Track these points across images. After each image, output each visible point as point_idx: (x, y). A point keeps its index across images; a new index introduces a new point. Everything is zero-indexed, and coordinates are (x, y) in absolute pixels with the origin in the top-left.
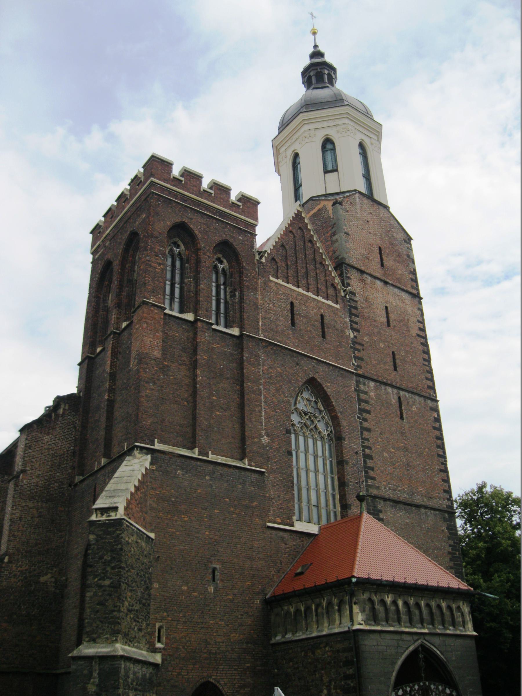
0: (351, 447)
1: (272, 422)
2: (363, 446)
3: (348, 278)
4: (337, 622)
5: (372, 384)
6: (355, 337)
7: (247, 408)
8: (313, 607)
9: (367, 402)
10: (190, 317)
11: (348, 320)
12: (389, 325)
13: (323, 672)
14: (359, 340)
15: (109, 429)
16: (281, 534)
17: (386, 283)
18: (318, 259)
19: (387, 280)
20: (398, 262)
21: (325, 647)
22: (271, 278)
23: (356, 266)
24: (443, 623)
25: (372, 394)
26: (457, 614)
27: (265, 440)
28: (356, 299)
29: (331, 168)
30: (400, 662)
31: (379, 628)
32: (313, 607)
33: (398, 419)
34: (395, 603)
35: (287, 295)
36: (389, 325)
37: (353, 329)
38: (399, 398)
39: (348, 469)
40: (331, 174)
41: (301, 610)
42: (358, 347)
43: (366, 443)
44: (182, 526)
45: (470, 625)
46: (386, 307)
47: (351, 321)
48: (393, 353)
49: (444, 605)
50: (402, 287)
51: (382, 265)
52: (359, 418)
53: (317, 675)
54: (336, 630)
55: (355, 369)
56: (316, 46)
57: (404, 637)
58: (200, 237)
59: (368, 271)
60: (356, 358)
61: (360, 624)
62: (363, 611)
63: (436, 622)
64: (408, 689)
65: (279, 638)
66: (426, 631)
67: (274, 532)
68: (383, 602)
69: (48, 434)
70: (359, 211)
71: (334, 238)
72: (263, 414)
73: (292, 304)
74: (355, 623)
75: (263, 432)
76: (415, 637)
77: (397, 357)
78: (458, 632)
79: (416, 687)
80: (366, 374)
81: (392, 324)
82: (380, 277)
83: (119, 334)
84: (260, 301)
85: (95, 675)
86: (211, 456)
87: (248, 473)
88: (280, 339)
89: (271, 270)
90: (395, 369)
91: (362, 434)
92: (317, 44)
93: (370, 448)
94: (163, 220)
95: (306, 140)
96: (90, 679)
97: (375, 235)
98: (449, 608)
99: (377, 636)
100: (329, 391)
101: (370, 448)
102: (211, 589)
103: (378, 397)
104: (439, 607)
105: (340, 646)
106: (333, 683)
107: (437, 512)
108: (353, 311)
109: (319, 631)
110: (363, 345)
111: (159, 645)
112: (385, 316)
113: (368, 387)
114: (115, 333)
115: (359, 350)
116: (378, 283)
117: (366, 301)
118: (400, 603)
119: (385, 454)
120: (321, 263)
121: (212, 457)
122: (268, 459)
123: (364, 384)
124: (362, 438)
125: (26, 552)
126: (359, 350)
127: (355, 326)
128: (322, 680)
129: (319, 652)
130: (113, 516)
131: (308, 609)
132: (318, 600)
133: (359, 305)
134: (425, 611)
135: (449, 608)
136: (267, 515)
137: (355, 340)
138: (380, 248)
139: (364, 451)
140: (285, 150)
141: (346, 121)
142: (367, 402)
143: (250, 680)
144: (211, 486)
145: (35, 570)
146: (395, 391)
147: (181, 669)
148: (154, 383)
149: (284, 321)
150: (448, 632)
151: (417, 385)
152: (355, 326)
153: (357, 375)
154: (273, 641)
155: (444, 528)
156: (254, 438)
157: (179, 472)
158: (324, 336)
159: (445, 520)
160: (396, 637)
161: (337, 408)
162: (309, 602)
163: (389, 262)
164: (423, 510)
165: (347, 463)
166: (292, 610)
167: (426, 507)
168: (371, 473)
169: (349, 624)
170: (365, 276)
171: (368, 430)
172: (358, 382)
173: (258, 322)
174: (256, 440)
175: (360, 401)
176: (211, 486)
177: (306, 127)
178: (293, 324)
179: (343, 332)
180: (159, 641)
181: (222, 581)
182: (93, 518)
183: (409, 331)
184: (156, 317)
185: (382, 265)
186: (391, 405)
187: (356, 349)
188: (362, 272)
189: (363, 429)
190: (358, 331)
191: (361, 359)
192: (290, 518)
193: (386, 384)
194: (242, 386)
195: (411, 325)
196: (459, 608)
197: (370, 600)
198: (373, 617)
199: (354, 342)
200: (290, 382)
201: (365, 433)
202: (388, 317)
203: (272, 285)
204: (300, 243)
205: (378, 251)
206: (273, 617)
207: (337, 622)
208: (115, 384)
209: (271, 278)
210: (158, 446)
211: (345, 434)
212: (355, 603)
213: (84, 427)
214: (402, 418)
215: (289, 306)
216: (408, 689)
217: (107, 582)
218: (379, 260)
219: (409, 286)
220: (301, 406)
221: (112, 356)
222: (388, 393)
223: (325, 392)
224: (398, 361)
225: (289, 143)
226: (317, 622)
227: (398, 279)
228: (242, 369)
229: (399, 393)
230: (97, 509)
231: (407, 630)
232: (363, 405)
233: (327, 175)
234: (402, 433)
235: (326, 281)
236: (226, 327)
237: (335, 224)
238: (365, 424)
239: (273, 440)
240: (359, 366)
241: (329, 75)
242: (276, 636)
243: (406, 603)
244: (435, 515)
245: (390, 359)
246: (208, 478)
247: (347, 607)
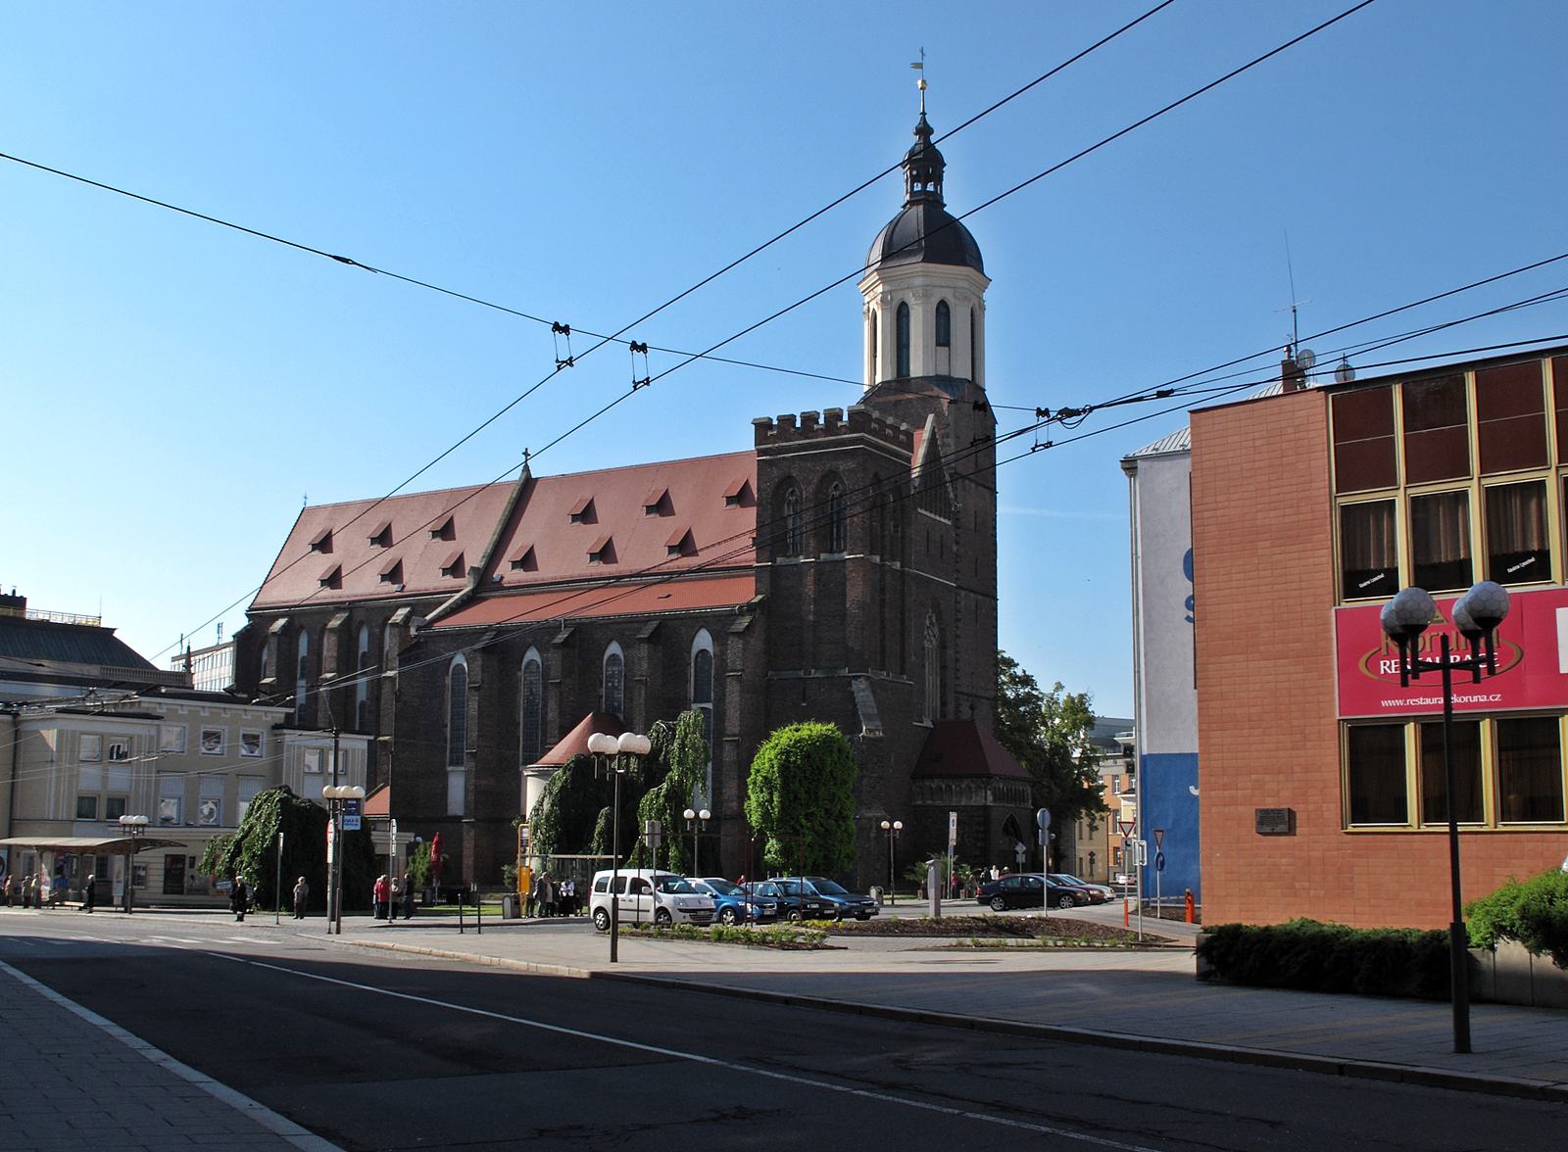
22: (919, 510)
25: (963, 603)
27: (913, 658)
29: (942, 341)
37: (957, 543)
42: (958, 560)
47: (956, 535)
56: (924, 113)
116: (973, 485)
142: (959, 611)
154: (913, 803)
168: (959, 675)
169: (983, 801)
175: (958, 611)
187: (957, 562)
192: (921, 716)
194: (902, 614)
198: (995, 800)
207: (974, 799)
209: (919, 510)
217: (875, 775)
228: (903, 601)
238: (958, 632)
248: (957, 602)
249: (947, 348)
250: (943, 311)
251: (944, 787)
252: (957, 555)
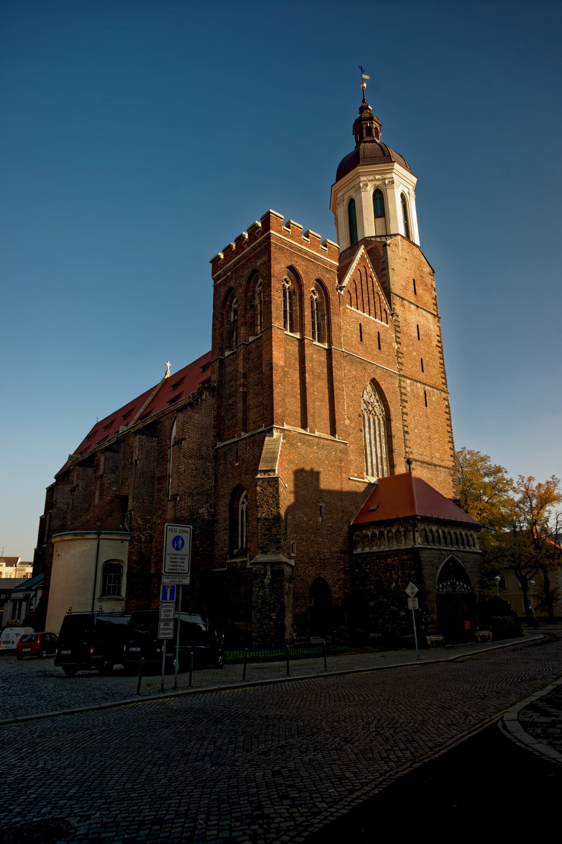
0: (396, 426)
1: (351, 409)
2: (403, 425)
3: (394, 303)
4: (404, 542)
5: (408, 381)
6: (398, 348)
7: (336, 400)
8: (386, 532)
9: (405, 395)
10: (298, 336)
11: (394, 335)
12: (419, 339)
13: (393, 572)
14: (400, 351)
15: (245, 412)
16: (358, 484)
17: (418, 307)
18: (375, 290)
19: (418, 305)
20: (425, 290)
21: (394, 557)
23: (398, 294)
24: (463, 545)
25: (409, 389)
26: (471, 539)
27: (347, 422)
28: (399, 320)
30: (440, 568)
31: (429, 547)
32: (386, 532)
33: (424, 407)
34: (437, 531)
35: (357, 318)
36: (419, 339)
38: (425, 392)
39: (395, 441)
40: (380, 219)
41: (376, 534)
42: (400, 355)
43: (405, 423)
44: (302, 480)
45: (477, 546)
46: (418, 326)
47: (396, 336)
48: (422, 359)
49: (463, 533)
50: (427, 310)
51: (415, 293)
52: (401, 406)
53: (388, 574)
54: (403, 547)
55: (399, 371)
57: (443, 552)
58: (303, 276)
59: (407, 299)
60: (399, 363)
61: (420, 544)
62: (421, 536)
63: (459, 544)
64: (445, 584)
65: (359, 550)
66: (454, 549)
67: (353, 483)
68: (431, 531)
69: (197, 413)
70: (400, 251)
71: (384, 273)
72: (345, 404)
73: (360, 325)
74: (417, 543)
75: (346, 417)
76: (449, 553)
77: (424, 362)
78: (471, 550)
79: (449, 583)
80: (405, 375)
81: (421, 338)
82: (413, 302)
83: (247, 345)
84: (342, 324)
85: (269, 573)
86: (316, 433)
87: (338, 444)
88: (354, 351)
89: (347, 300)
90: (423, 371)
91: (402, 417)
93: (407, 426)
94: (280, 263)
96: (265, 577)
97: (411, 269)
98: (466, 535)
99: (428, 551)
100: (383, 387)
101: (407, 426)
102: (320, 520)
103: (412, 391)
104: (461, 534)
105: (405, 557)
106: (400, 579)
107: (446, 470)
108: (397, 329)
109: (390, 547)
110: (403, 354)
111: (293, 555)
112: (417, 332)
113: (406, 384)
114: (244, 344)
115: (400, 358)
116: (412, 306)
117: (405, 321)
118: (440, 531)
119: (416, 431)
120: (377, 293)
121: (317, 434)
122: (349, 435)
123: (404, 382)
124: (403, 420)
125: (190, 493)
126: (400, 358)
127: (398, 340)
128: (392, 578)
129: (389, 561)
130: (272, 475)
131: (381, 533)
132: (389, 528)
133: (400, 325)
134: (453, 536)
135: (466, 535)
136: (349, 472)
137: (399, 350)
138: (414, 280)
139: (403, 428)
142: (405, 395)
143: (342, 576)
144: (317, 453)
145: (195, 505)
146: (423, 386)
147: (305, 569)
148: (282, 384)
149: (356, 337)
150: (466, 550)
151: (436, 382)
152: (398, 340)
153: (400, 375)
154: (355, 552)
155: (450, 481)
156: (340, 421)
157: (299, 444)
158: (380, 348)
159: (451, 475)
160: (438, 552)
161: (388, 399)
162: (382, 529)
163: (419, 291)
164: (438, 468)
165: (394, 437)
166: (369, 534)
167: (440, 466)
169: (413, 544)
170: (405, 302)
171: (406, 414)
172: (400, 380)
173: (340, 339)
174: (342, 422)
175: (402, 393)
176: (317, 453)
178: (361, 340)
179: (391, 344)
180: (292, 552)
181: (326, 514)
182: (259, 476)
183: (431, 343)
184: (280, 336)
185: (415, 293)
186: (420, 396)
188: (403, 299)
189: (404, 413)
190: (400, 343)
191: (402, 364)
192: (362, 473)
193: (417, 381)
195: (433, 338)
196: (471, 535)
197: (425, 529)
199: (398, 352)
200: (360, 381)
201: (405, 416)
202: (418, 333)
203: (348, 311)
204: (364, 278)
205: (413, 282)
206: (354, 537)
207: (404, 542)
208: (246, 381)
210: (286, 427)
211: (393, 417)
212: (417, 531)
213: (219, 407)
214: (426, 405)
215: (359, 326)
216: (445, 584)
218: (413, 290)
219: (432, 309)
220: (366, 397)
221: (243, 361)
222: (418, 388)
223: (381, 388)
224: (424, 365)
225: (346, 190)
226: (388, 541)
227: (425, 304)
229: (425, 388)
230: (261, 471)
231: (444, 548)
232: (404, 397)
233: (376, 219)
234: (426, 416)
235: (380, 306)
236: (319, 342)
237: (384, 261)
238: (405, 410)
239: (351, 422)
240: (401, 369)
242: (356, 549)
243: (443, 532)
244: (445, 472)
245: (419, 364)
246: (315, 447)
247: (411, 533)
248: (400, 386)
249: (383, 219)
251: (377, 533)
252: (398, 352)
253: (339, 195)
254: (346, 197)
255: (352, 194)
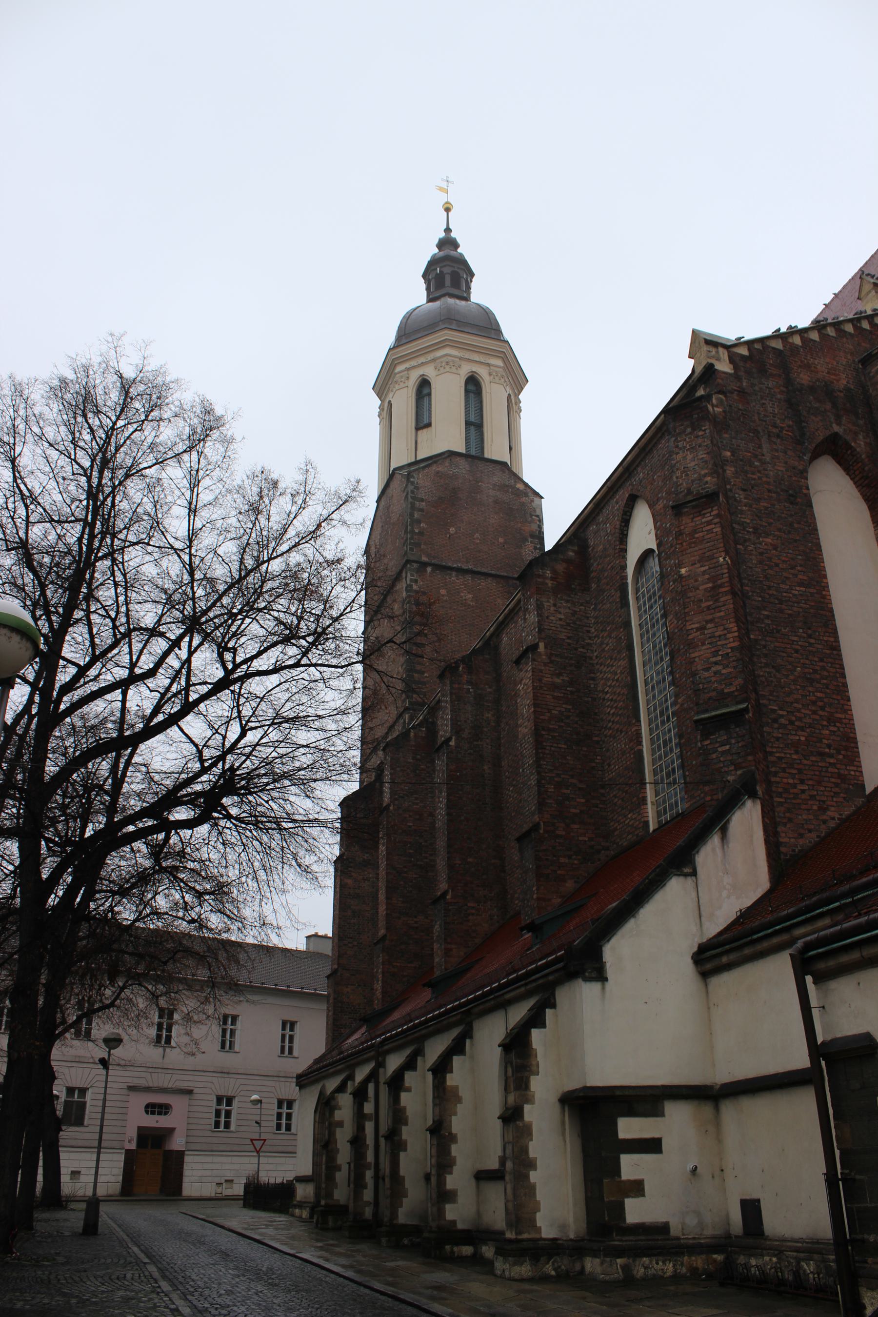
56: (448, 230)
92: (450, 227)
95: (447, 368)
140: (408, 369)
141: (499, 363)
177: (447, 351)
241: (466, 281)
250: (473, 386)
253: (399, 369)
254: (414, 377)
255: (429, 372)
